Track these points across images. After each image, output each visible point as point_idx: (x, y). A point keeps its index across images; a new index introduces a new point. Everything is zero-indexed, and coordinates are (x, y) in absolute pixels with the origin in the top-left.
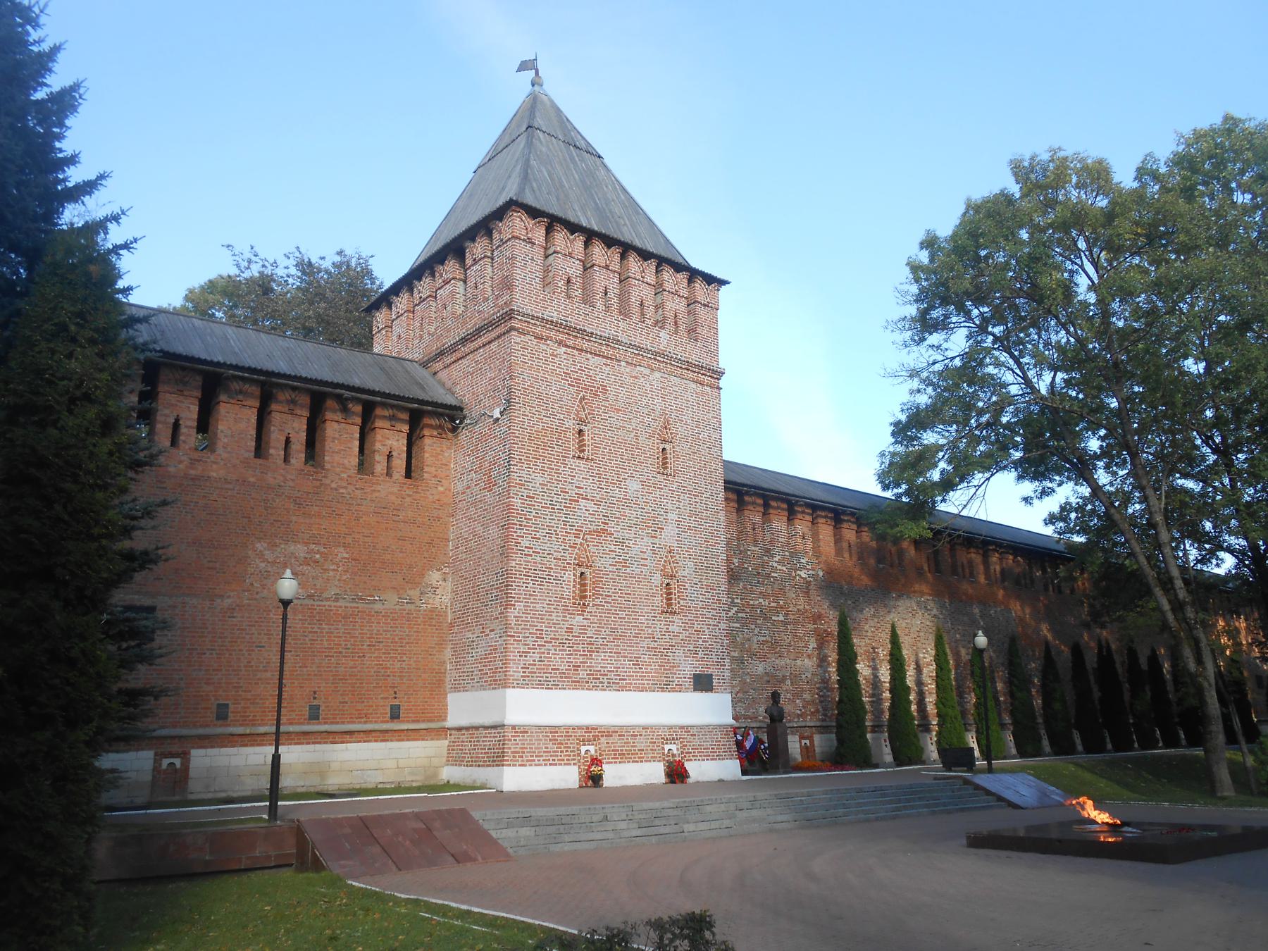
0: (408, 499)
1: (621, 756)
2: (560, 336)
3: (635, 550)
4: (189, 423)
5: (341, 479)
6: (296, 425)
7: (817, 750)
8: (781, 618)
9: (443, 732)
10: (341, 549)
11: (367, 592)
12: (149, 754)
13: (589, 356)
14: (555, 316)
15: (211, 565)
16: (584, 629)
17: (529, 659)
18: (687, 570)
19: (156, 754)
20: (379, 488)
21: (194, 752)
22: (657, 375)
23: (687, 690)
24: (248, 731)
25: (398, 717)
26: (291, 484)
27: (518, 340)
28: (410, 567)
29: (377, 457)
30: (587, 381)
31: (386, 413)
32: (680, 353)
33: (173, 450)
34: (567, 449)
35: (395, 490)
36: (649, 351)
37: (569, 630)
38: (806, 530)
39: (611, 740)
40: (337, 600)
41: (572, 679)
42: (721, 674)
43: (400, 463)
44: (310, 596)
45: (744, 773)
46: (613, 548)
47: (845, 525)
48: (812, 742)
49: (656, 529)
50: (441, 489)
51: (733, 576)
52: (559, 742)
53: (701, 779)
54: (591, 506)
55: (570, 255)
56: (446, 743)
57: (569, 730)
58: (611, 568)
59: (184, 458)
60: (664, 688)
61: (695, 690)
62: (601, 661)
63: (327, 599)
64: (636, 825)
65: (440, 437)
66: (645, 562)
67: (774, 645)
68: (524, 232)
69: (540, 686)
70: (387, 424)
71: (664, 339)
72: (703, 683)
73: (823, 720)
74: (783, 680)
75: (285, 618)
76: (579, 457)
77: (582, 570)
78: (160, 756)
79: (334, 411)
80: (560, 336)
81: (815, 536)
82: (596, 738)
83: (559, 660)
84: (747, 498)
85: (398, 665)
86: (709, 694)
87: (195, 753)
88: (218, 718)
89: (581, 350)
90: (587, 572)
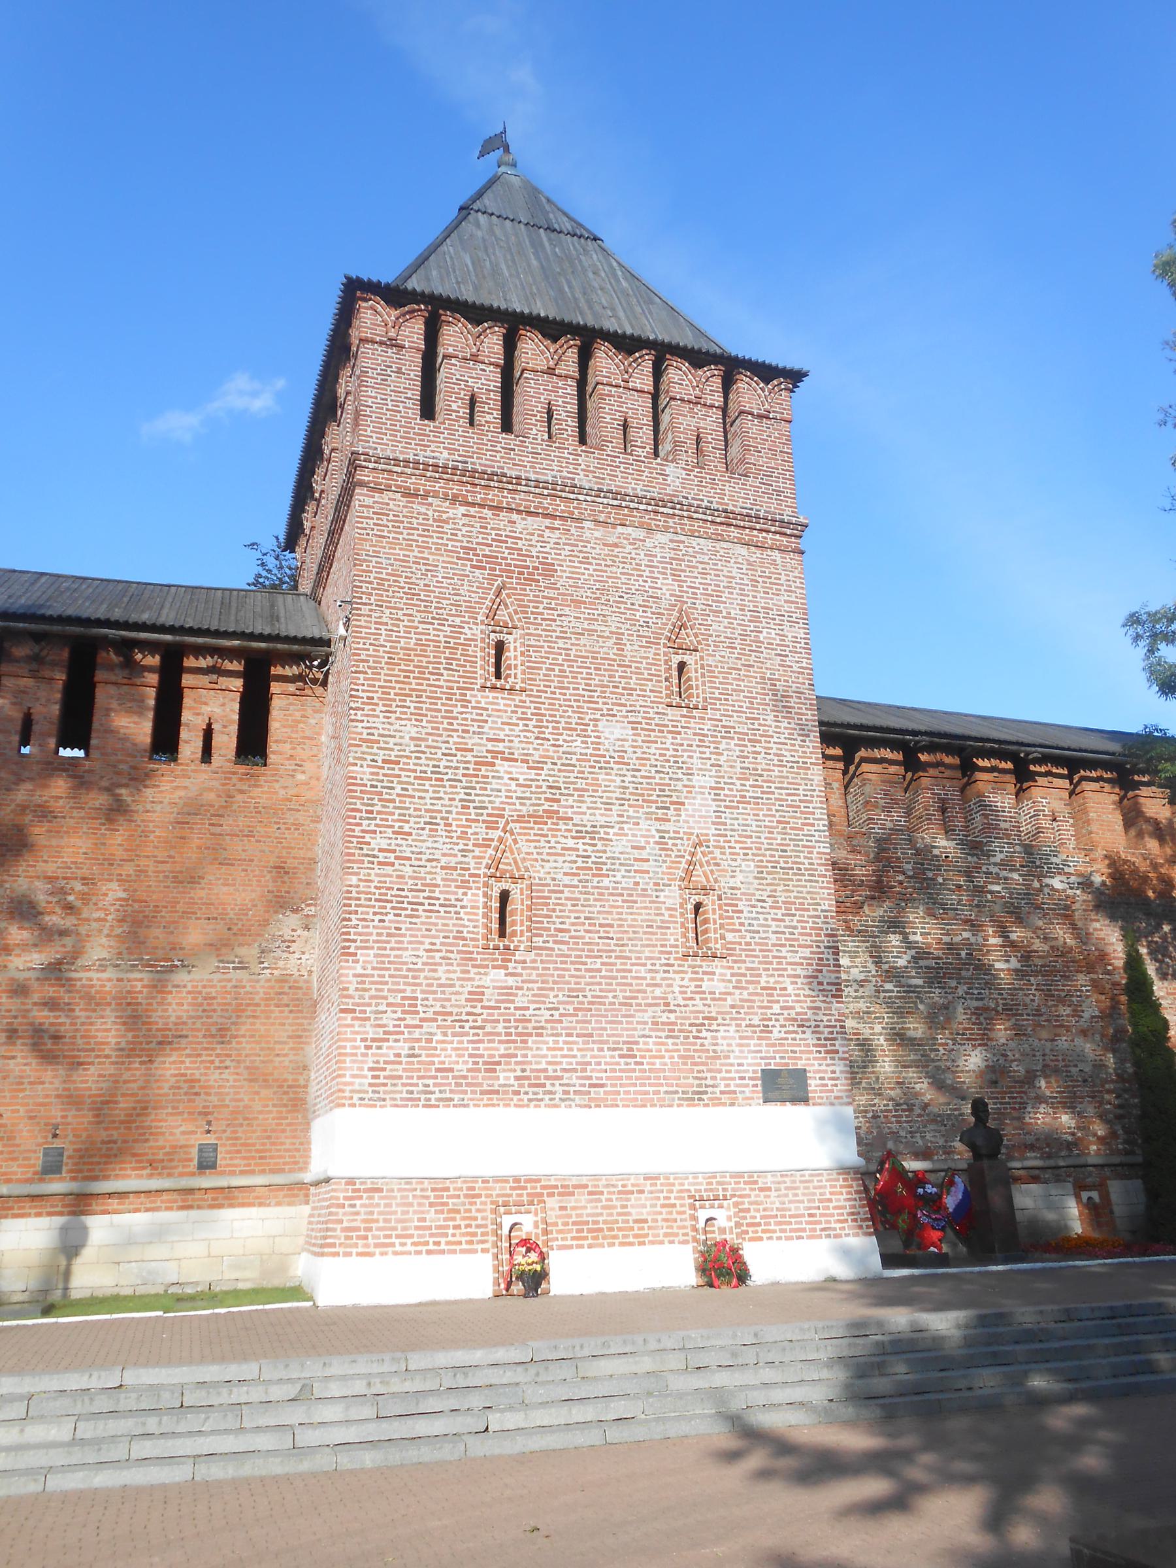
1: (593, 1234)
2: (455, 489)
3: (619, 846)
5: (118, 773)
7: (1118, 1210)
9: (299, 1191)
13: (515, 516)
14: (443, 457)
16: (508, 994)
17: (388, 1051)
18: (739, 876)
27: (369, 501)
29: (184, 734)
30: (512, 559)
31: (203, 663)
32: (708, 497)
34: (470, 676)
35: (216, 784)
36: (640, 499)
37: (476, 996)
38: (1058, 806)
39: (571, 1202)
42: (824, 1073)
45: (889, 1260)
46: (571, 843)
47: (1145, 791)
48: (1105, 1196)
49: (667, 804)
50: (300, 777)
53: (558, 1293)
54: (521, 772)
55: (474, 358)
56: (306, 1210)
57: (472, 1188)
58: (567, 880)
60: (696, 1098)
62: (542, 1053)
64: (368, 1412)
65: (300, 694)
66: (645, 866)
68: (380, 330)
69: (411, 1101)
70: (204, 680)
71: (675, 477)
72: (783, 1086)
73: (1127, 1153)
76: (494, 688)
77: (504, 885)
79: (111, 668)
80: (455, 489)
81: (1080, 817)
82: (536, 1199)
83: (453, 1053)
84: (924, 757)
86: (800, 1109)
89: (499, 508)
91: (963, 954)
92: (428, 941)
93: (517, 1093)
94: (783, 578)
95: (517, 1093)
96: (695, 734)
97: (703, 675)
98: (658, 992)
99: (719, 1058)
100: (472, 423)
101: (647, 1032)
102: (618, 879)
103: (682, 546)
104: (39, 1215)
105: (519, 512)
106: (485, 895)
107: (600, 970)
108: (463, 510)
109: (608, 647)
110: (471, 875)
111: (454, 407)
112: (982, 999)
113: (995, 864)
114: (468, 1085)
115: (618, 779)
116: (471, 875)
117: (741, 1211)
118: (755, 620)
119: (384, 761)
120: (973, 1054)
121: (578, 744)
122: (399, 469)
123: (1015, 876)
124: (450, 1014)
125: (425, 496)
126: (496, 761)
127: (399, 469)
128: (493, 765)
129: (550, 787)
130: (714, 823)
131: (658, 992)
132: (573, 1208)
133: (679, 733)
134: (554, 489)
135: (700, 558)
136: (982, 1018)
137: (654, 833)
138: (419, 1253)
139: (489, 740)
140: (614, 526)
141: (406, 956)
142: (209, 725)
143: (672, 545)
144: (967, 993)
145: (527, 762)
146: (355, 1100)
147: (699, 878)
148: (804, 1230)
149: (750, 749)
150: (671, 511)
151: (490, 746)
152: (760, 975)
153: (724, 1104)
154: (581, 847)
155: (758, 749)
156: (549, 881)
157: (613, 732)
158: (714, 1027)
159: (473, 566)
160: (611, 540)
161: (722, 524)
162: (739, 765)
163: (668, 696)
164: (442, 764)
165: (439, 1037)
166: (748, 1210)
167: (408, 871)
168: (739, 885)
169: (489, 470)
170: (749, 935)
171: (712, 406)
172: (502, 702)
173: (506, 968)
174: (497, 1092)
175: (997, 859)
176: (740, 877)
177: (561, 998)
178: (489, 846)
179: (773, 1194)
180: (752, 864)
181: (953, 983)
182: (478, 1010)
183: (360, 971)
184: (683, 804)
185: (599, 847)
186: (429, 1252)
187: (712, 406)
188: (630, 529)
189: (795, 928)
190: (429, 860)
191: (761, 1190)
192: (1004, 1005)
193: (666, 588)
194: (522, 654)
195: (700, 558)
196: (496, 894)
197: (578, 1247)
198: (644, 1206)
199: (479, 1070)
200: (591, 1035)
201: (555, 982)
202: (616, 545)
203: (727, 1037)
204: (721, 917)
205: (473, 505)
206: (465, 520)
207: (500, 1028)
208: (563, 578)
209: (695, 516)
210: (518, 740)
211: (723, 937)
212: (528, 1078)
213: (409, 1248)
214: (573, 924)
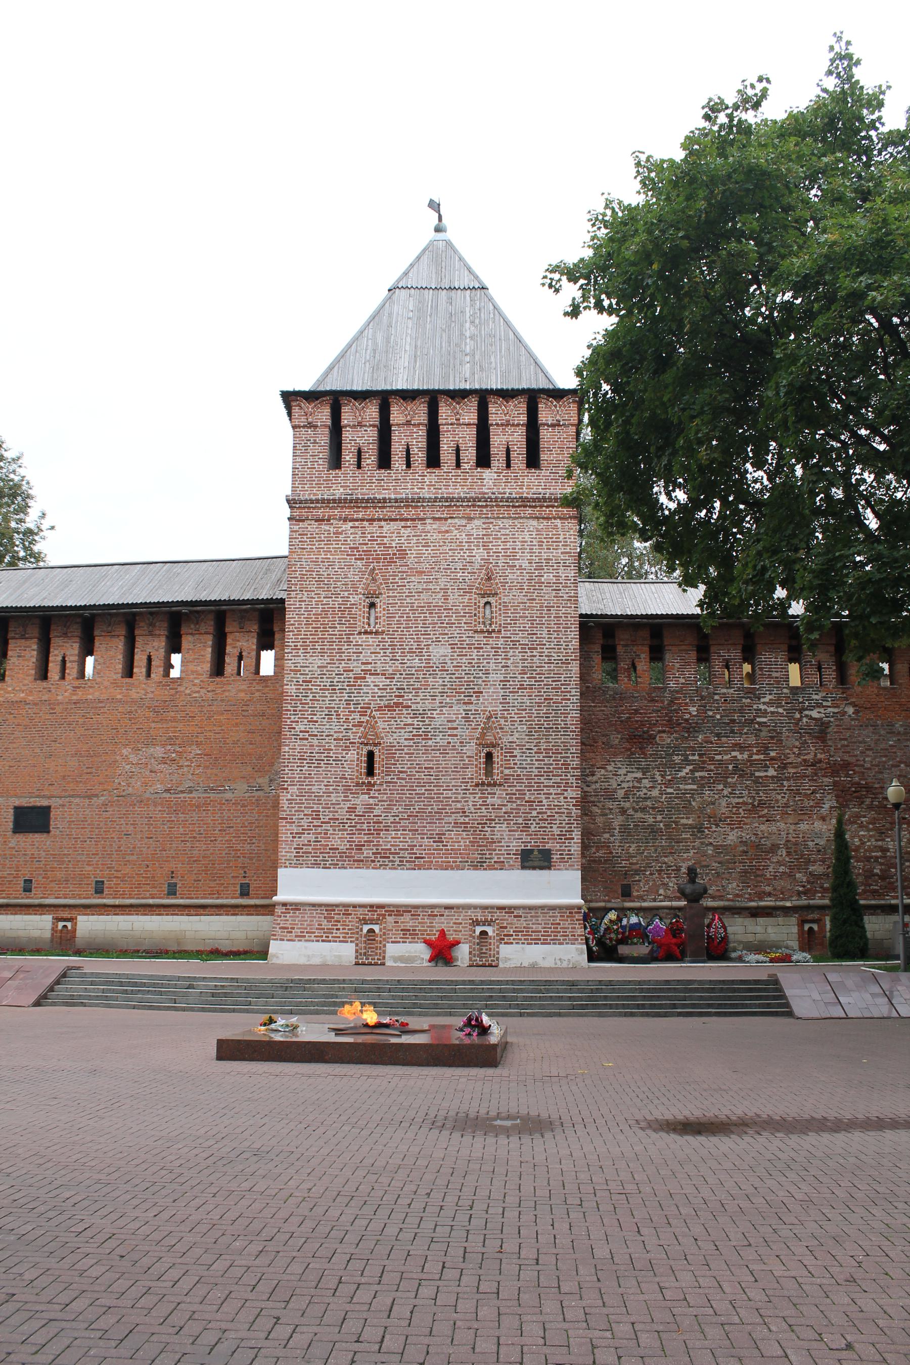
0: (257, 694)
3: (440, 720)
4: (72, 658)
6: (156, 644)
8: (771, 772)
10: (194, 747)
11: (218, 783)
13: (383, 523)
14: (339, 492)
15: (89, 770)
16: (370, 808)
17: (305, 838)
18: (514, 735)
19: (53, 918)
20: (229, 687)
21: (80, 918)
22: (476, 522)
23: (511, 868)
24: (117, 903)
25: (102, 892)
26: (151, 695)
28: (260, 758)
30: (379, 550)
32: (511, 490)
33: (62, 682)
34: (353, 626)
35: (244, 687)
36: (463, 500)
37: (352, 810)
39: (401, 919)
40: (191, 792)
41: (350, 858)
44: (168, 791)
46: (410, 721)
49: (469, 692)
52: (332, 918)
54: (381, 681)
55: (360, 425)
58: (406, 743)
59: (68, 687)
60: (478, 865)
62: (388, 840)
63: (182, 792)
66: (455, 732)
67: (754, 809)
69: (316, 865)
72: (535, 859)
74: (774, 848)
85: (247, 847)
87: (80, 918)
88: (96, 892)
89: (373, 520)
90: (376, 751)
91: (730, 767)
92: (326, 780)
93: (373, 861)
94: (562, 537)
95: (373, 861)
96: (492, 648)
97: (500, 609)
98: (459, 805)
99: (495, 842)
100: (359, 466)
101: (450, 828)
102: (438, 740)
103: (491, 526)
104: (167, 915)
105: (385, 520)
106: (358, 754)
107: (424, 794)
108: (351, 524)
109: (438, 599)
110: (351, 743)
111: (348, 458)
112: (742, 797)
113: (764, 703)
114: (346, 857)
115: (441, 680)
116: (351, 743)
117: (501, 927)
119: (303, 681)
120: (731, 834)
121: (417, 661)
122: (313, 505)
123: (780, 710)
124: (338, 819)
125: (328, 520)
126: (367, 676)
127: (313, 505)
128: (365, 678)
129: (398, 689)
130: (501, 703)
131: (459, 805)
132: (402, 922)
133: (482, 648)
135: (503, 532)
136: (741, 810)
137: (462, 711)
138: (318, 941)
139: (363, 663)
140: (446, 519)
141: (314, 789)
142: (241, 653)
143: (484, 526)
144: (730, 793)
145: (385, 674)
146: (287, 864)
147: (490, 738)
148: (540, 939)
149: (529, 654)
150: (484, 504)
151: (363, 667)
152: (525, 794)
153: (496, 869)
154: (416, 723)
155: (535, 654)
156: (395, 744)
158: (493, 825)
159: (356, 559)
160: (443, 529)
161: (519, 507)
162: (520, 665)
163: (475, 626)
164: (335, 680)
165: (331, 832)
166: (506, 927)
167: (316, 742)
168: (515, 740)
169: (366, 497)
170: (519, 770)
171: (518, 425)
172: (371, 640)
173: (369, 794)
174: (362, 861)
176: (516, 735)
177: (400, 810)
178: (361, 726)
179: (523, 919)
180: (525, 727)
181: (721, 787)
182: (353, 817)
183: (289, 797)
184: (482, 692)
185: (427, 723)
186: (323, 941)
187: (518, 425)
188: (456, 520)
189: (552, 764)
190: (327, 736)
191: (515, 917)
192: (760, 801)
193: (479, 554)
194: (384, 609)
195: (503, 532)
196: (365, 752)
197: (403, 942)
198: (443, 923)
199: (353, 849)
200: (417, 830)
201: (397, 801)
202: (447, 532)
204: (502, 760)
205: (357, 520)
206: (352, 530)
207: (365, 826)
208: (411, 559)
209: (501, 504)
211: (502, 772)
212: (380, 853)
213: (313, 938)
214: (409, 768)
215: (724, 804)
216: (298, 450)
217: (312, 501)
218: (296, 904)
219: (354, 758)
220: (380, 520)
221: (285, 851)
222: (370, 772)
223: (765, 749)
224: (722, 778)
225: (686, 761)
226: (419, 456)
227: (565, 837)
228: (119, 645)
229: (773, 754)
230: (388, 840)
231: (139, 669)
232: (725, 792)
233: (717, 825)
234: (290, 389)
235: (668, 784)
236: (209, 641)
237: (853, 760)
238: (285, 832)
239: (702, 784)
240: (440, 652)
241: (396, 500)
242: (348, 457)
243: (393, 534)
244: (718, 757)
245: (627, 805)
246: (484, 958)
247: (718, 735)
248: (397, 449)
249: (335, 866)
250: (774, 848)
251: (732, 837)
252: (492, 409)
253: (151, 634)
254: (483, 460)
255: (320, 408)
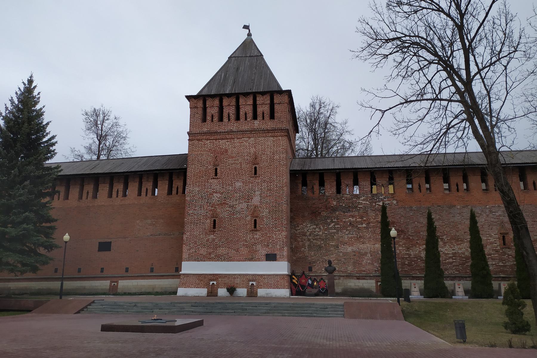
3: (238, 208)
8: (364, 225)
12: (109, 281)
18: (265, 213)
22: (252, 139)
32: (264, 127)
37: (208, 240)
43: (180, 190)
45: (292, 294)
46: (228, 209)
49: (249, 198)
51: (291, 212)
54: (219, 195)
55: (213, 106)
60: (251, 260)
61: (267, 260)
69: (195, 260)
72: (271, 257)
74: (366, 254)
75: (66, 246)
78: (112, 282)
100: (212, 121)
118: (273, 154)
123: (367, 202)
134: (228, 133)
157: (238, 184)
175: (362, 199)
193: (253, 150)
203: (259, 247)
208: (229, 152)
210: (218, 188)
215: (346, 237)
216: (192, 116)
217: (196, 134)
218: (188, 274)
219: (208, 222)
220: (219, 139)
221: (185, 255)
222: (214, 227)
223: (362, 217)
224: (345, 227)
225: (332, 222)
226: (233, 117)
227: (282, 249)
228: (137, 185)
229: (365, 219)
230: (221, 251)
231: (143, 193)
232: (347, 233)
233: (344, 245)
234: (188, 95)
235: (326, 230)
236: (167, 182)
237: (396, 221)
238: (185, 248)
239: (338, 230)
240: (238, 184)
241: (224, 132)
242: (209, 118)
243: (223, 144)
244: (344, 220)
245: (311, 238)
246: (252, 293)
247: (344, 212)
248: (225, 115)
249: (202, 260)
250: (366, 254)
251: (350, 249)
252: (258, 99)
253: (147, 181)
254: (255, 117)
255: (199, 101)
